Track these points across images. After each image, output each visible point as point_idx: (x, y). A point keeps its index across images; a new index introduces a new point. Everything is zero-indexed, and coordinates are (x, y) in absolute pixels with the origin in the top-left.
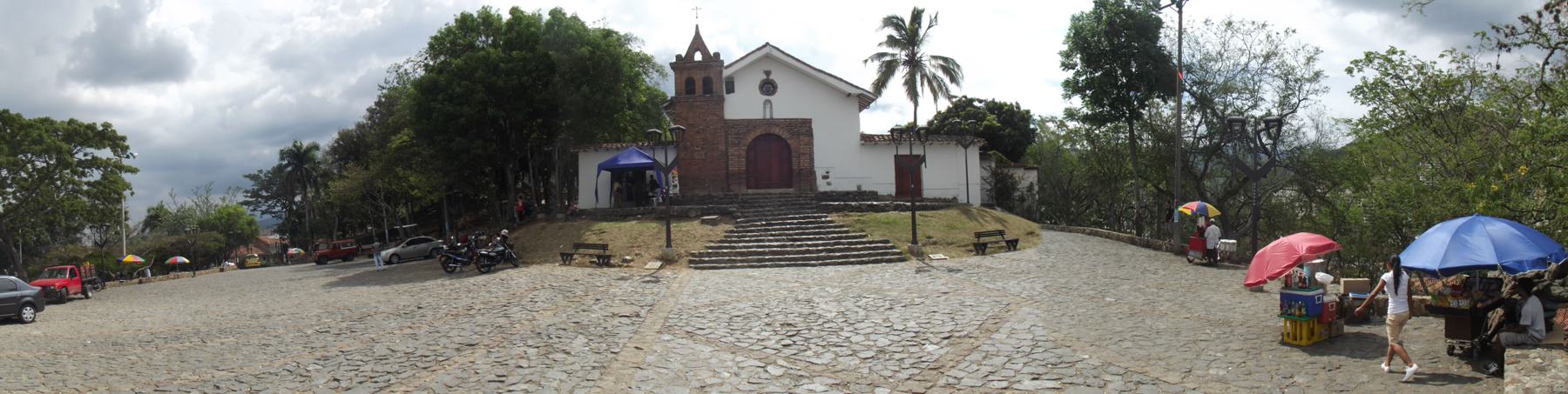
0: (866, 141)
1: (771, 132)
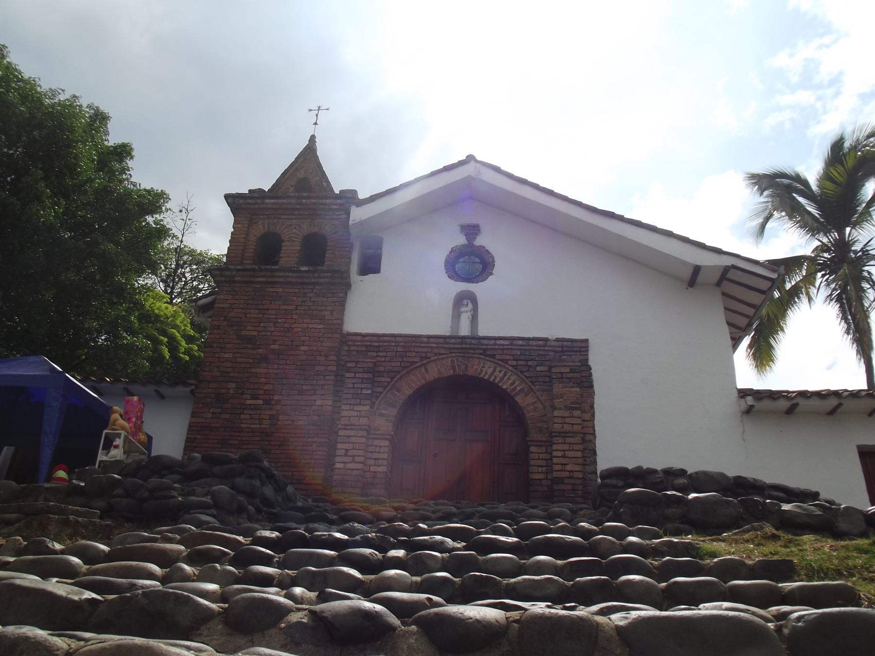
1: (471, 372)
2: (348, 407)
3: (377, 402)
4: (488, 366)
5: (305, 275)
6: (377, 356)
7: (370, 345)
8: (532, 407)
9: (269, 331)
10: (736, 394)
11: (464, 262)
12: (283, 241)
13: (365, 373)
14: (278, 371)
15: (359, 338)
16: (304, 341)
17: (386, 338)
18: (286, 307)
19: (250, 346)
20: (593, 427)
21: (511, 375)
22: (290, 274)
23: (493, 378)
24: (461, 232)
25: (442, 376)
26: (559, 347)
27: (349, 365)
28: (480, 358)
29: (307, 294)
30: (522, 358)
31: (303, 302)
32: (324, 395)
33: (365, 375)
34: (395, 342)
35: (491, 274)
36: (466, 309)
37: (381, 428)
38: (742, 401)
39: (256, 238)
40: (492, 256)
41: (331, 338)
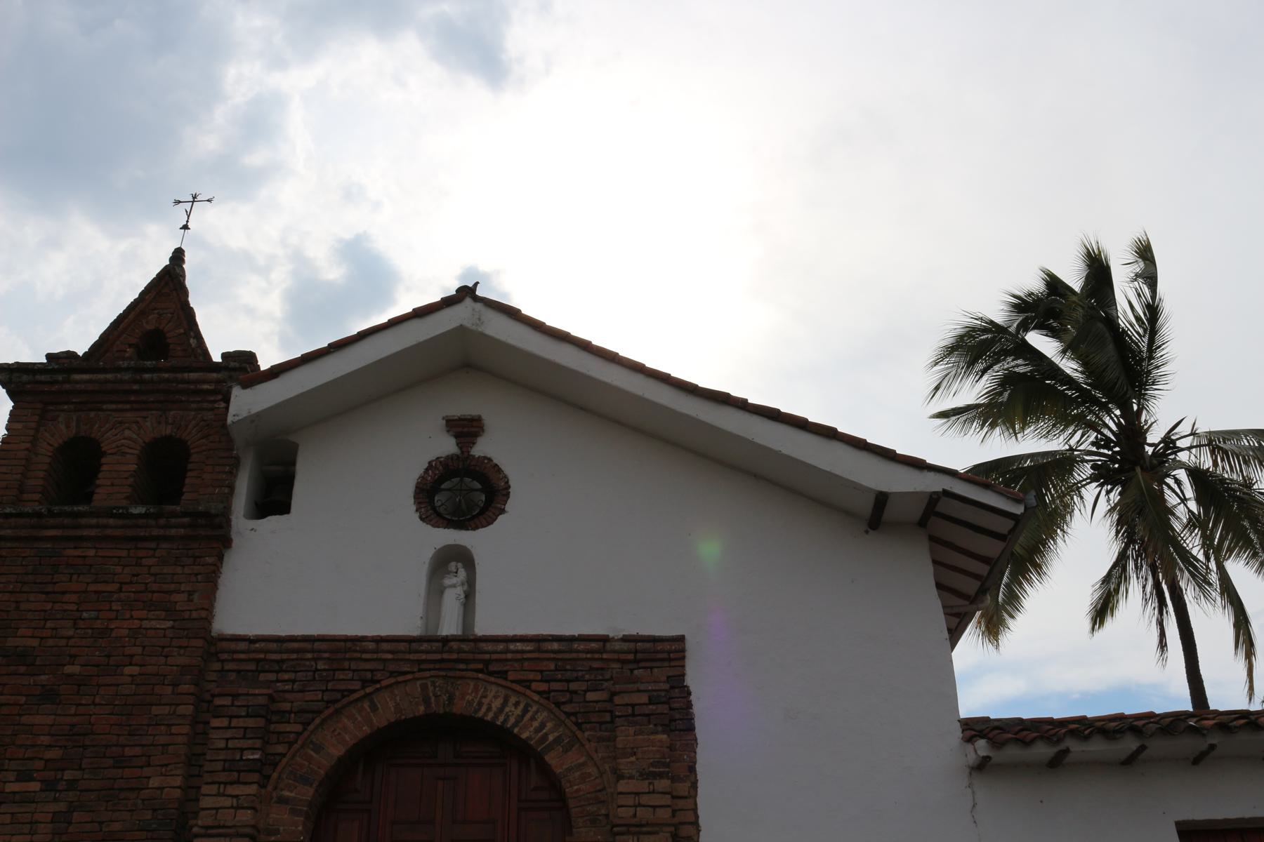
0: (996, 744)
1: (459, 707)
2: (213, 789)
3: (275, 775)
4: (493, 694)
5: (141, 521)
6: (278, 681)
7: (264, 660)
8: (577, 774)
9: (62, 638)
10: (958, 732)
11: (449, 490)
12: (104, 454)
13: (251, 717)
14: (75, 720)
15: (243, 645)
16: (132, 656)
17: (296, 645)
18: (100, 587)
19: (23, 669)
20: (695, 810)
21: (537, 712)
22: (111, 521)
23: (502, 718)
24: (448, 431)
25: (403, 717)
26: (629, 652)
27: (218, 701)
28: (478, 679)
29: (144, 560)
30: (560, 676)
31: (134, 575)
32: (166, 765)
33: (251, 722)
34: (313, 651)
35: (503, 511)
36: (454, 580)
37: (281, 828)
38: (969, 747)
39: (51, 449)
40: (506, 477)
41: (187, 647)
